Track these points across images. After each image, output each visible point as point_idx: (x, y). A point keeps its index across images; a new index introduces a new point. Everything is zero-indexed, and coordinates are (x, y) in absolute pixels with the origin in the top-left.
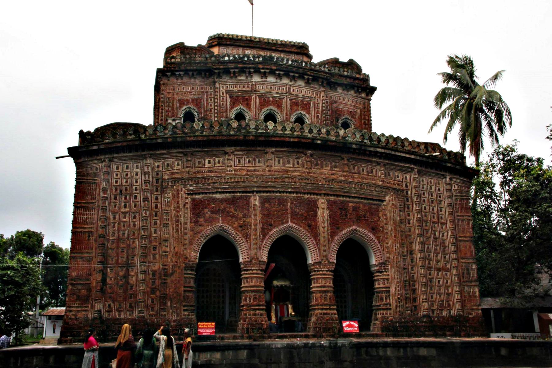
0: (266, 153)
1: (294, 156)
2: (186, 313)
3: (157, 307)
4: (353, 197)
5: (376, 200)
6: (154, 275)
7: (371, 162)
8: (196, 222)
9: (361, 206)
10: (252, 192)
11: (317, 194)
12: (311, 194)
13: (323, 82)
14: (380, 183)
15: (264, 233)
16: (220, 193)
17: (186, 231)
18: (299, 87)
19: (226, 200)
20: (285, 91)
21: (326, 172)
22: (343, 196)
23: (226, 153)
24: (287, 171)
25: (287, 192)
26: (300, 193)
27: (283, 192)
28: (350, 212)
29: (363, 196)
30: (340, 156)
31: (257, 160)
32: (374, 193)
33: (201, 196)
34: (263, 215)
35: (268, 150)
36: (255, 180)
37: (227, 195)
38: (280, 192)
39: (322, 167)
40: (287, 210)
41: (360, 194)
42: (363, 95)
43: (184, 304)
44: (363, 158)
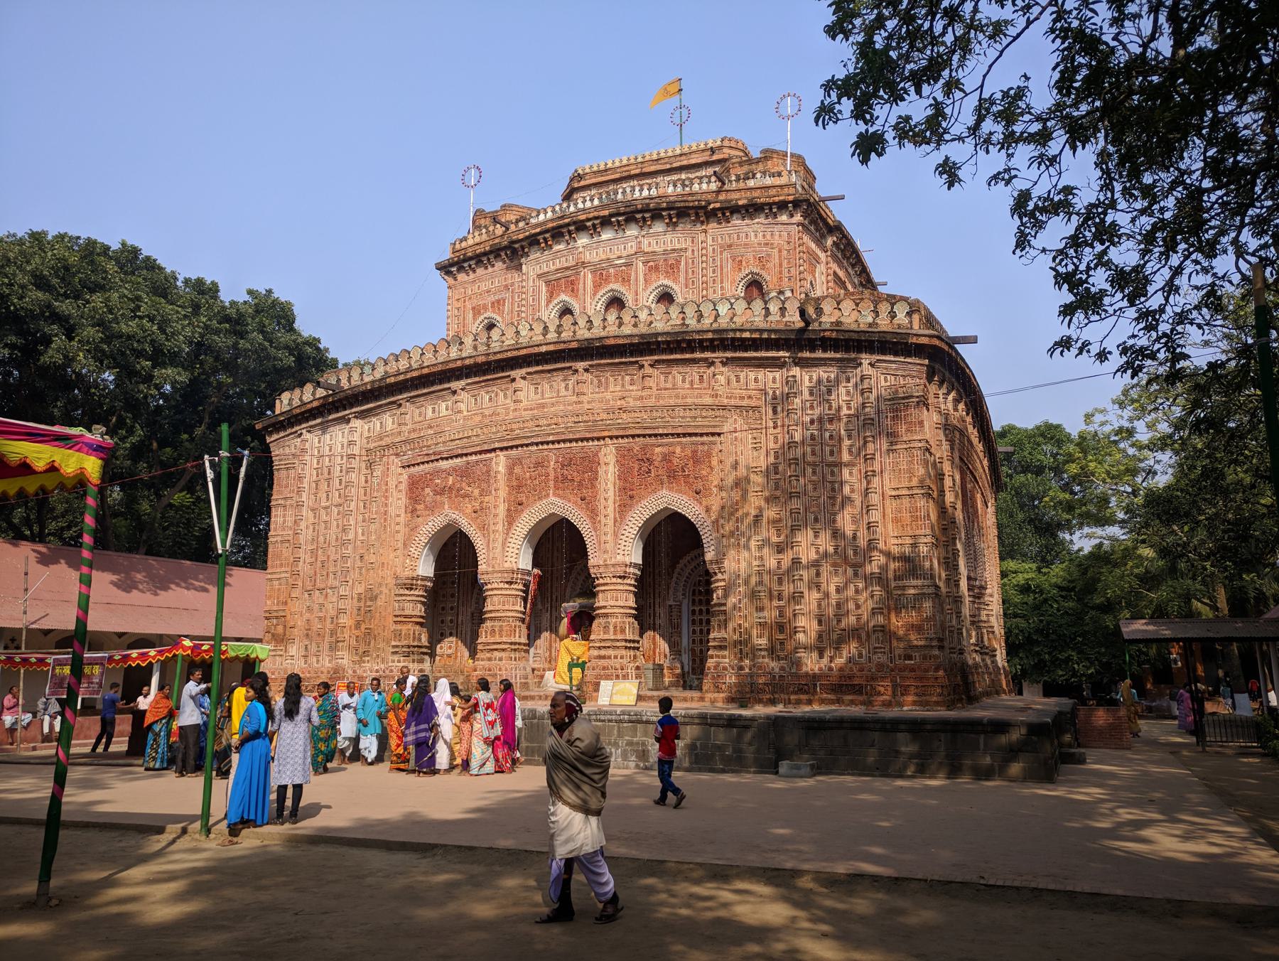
0: (514, 380)
1: (559, 377)
2: (396, 658)
3: (361, 651)
4: (661, 435)
5: (707, 434)
6: (359, 600)
7: (694, 361)
8: (414, 511)
9: (678, 450)
10: (494, 450)
11: (598, 439)
12: (587, 439)
13: (697, 214)
14: (708, 400)
15: (511, 520)
16: (447, 459)
17: (397, 528)
18: (657, 234)
19: (454, 470)
20: (634, 250)
21: (608, 396)
22: (644, 436)
23: (454, 392)
24: (543, 406)
25: (547, 443)
26: (570, 441)
27: (542, 443)
28: (656, 463)
29: (680, 431)
30: (637, 362)
31: (501, 394)
32: (700, 422)
33: (422, 467)
34: (511, 487)
35: (513, 373)
36: (494, 430)
37: (459, 460)
38: (537, 444)
39: (607, 388)
40: (547, 475)
41: (674, 427)
42: (784, 218)
43: (393, 643)
44: (678, 356)
